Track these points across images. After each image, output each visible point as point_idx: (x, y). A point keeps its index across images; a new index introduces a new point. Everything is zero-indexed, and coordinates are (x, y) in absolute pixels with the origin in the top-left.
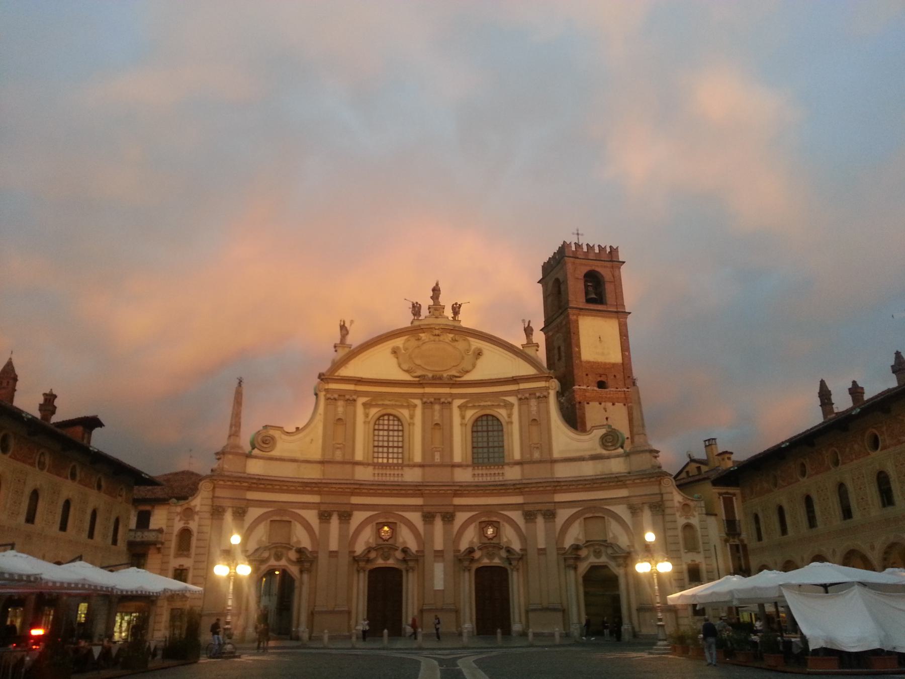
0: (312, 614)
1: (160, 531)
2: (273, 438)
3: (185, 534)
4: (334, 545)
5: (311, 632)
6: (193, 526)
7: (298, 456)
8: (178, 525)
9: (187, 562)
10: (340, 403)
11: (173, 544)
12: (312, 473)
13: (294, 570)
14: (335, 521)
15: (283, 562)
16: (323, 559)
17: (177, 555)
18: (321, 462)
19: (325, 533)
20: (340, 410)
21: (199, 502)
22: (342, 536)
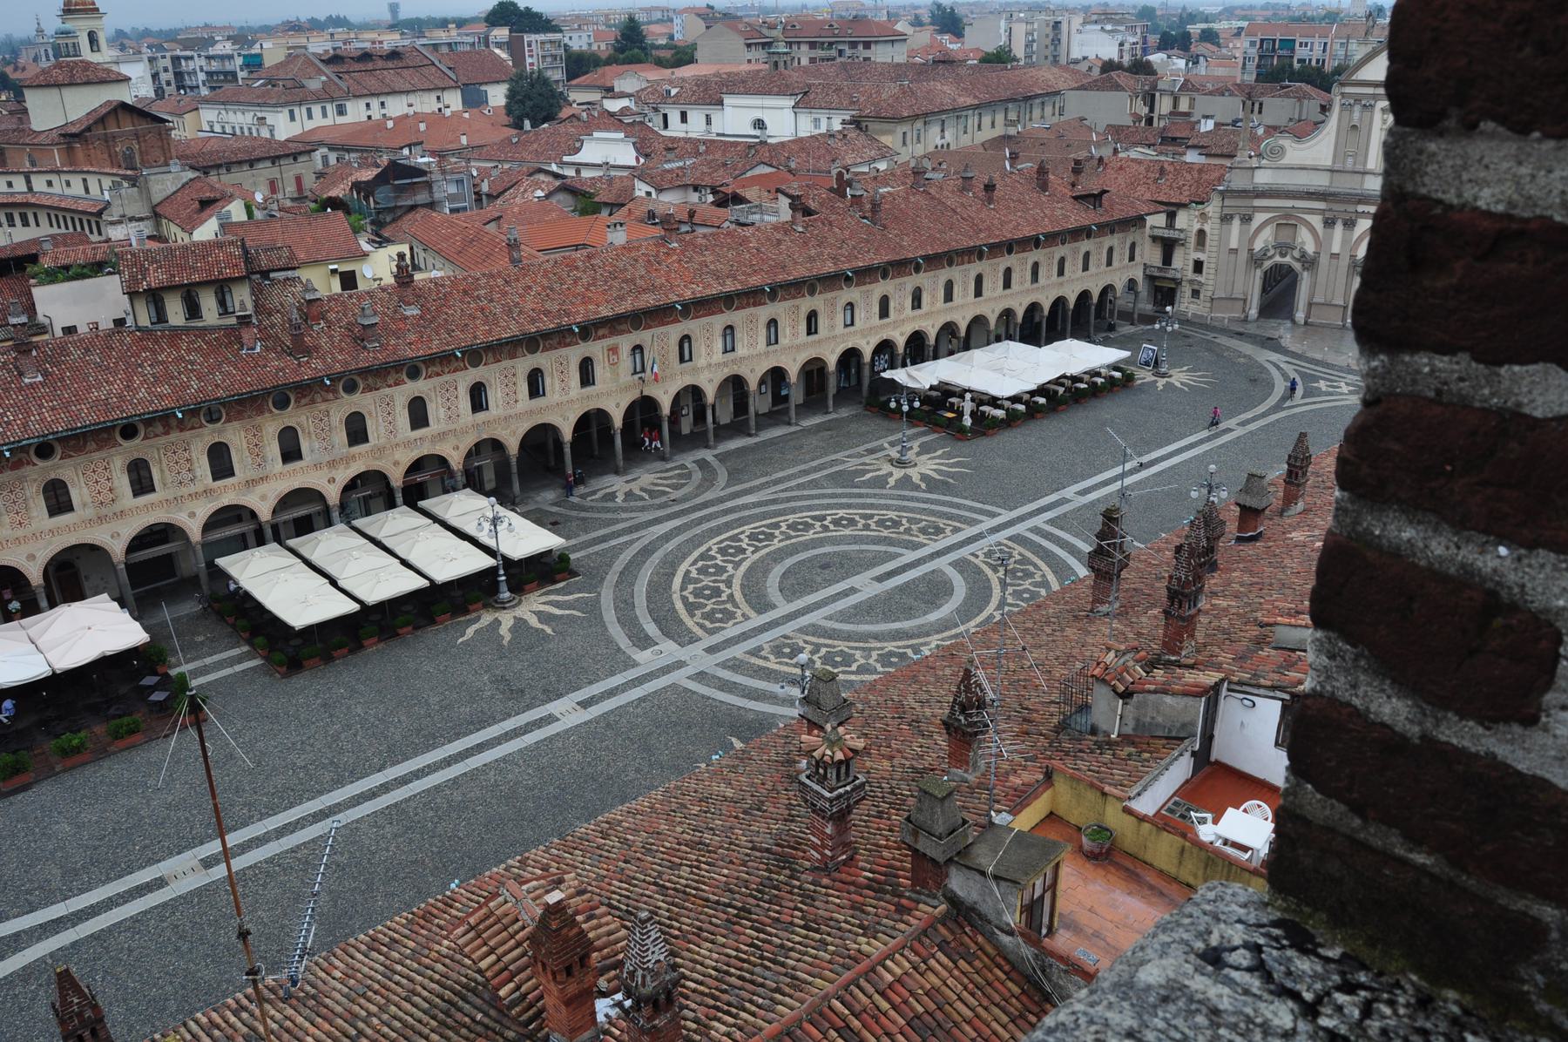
0: (1310, 305)
1: (1181, 231)
2: (1282, 148)
3: (1201, 233)
4: (1336, 249)
5: (1308, 316)
6: (1207, 228)
7: (1308, 162)
8: (1197, 226)
9: (1201, 256)
10: (1357, 108)
11: (1193, 240)
12: (1321, 181)
13: (1297, 266)
14: (1339, 227)
15: (1288, 259)
16: (1324, 260)
17: (1196, 250)
18: (1332, 171)
19: (1330, 239)
20: (1356, 115)
21: (1213, 208)
22: (1344, 242)
